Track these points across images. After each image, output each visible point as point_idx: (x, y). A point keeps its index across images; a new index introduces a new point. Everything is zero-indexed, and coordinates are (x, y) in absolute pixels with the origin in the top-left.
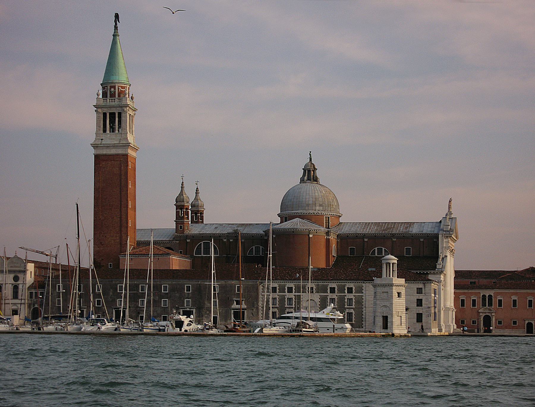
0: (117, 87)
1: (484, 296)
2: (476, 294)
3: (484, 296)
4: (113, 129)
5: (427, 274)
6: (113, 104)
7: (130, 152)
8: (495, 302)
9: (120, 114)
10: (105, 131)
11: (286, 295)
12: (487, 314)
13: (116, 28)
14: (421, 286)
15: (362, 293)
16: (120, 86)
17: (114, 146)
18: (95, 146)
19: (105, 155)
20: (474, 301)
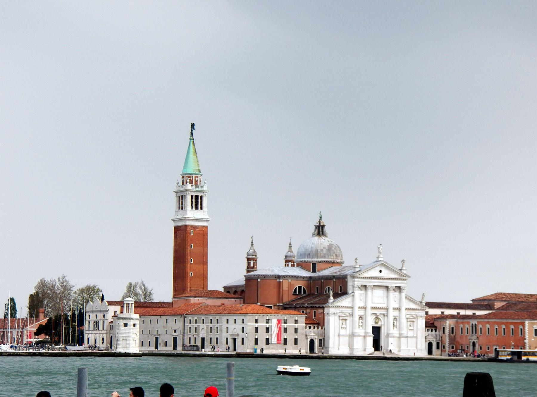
0: (185, 177)
1: (472, 324)
2: (468, 323)
3: (472, 324)
4: (182, 209)
5: (323, 308)
6: (182, 189)
7: (188, 223)
10: (179, 209)
11: (194, 325)
12: (473, 340)
13: (192, 134)
14: (243, 317)
15: (221, 323)
16: (188, 176)
18: (174, 220)
20: (467, 328)
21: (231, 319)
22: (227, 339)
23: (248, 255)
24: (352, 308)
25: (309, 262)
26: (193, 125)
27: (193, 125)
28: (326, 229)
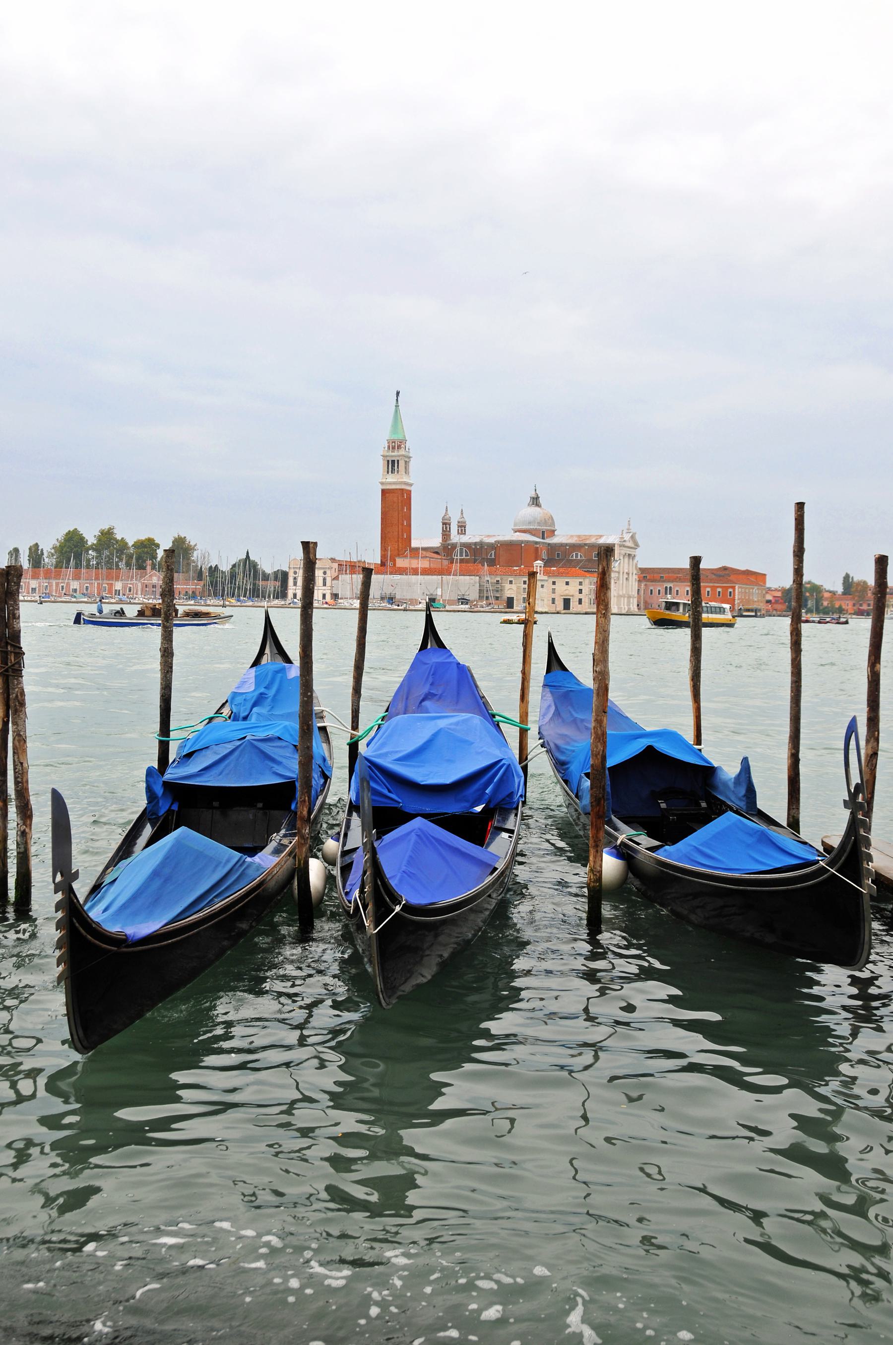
1: (666, 587)
2: (660, 585)
3: (666, 587)
6: (393, 454)
8: (674, 591)
9: (398, 461)
10: (388, 472)
13: (397, 400)
17: (394, 483)
18: (382, 483)
19: (389, 489)
20: (659, 590)
21: (560, 582)
22: (553, 600)
23: (443, 519)
24: (619, 573)
25: (539, 530)
26: (398, 393)
27: (398, 393)
28: (541, 500)
